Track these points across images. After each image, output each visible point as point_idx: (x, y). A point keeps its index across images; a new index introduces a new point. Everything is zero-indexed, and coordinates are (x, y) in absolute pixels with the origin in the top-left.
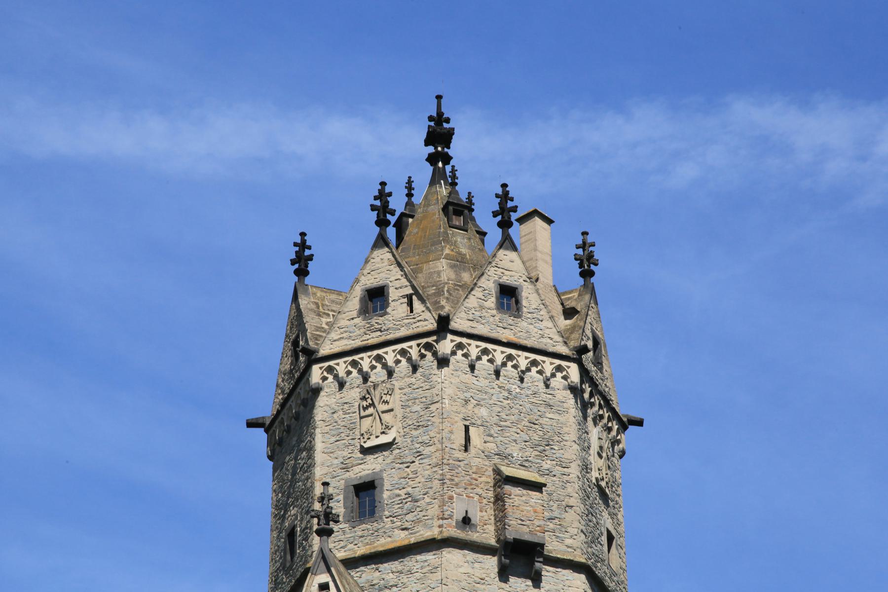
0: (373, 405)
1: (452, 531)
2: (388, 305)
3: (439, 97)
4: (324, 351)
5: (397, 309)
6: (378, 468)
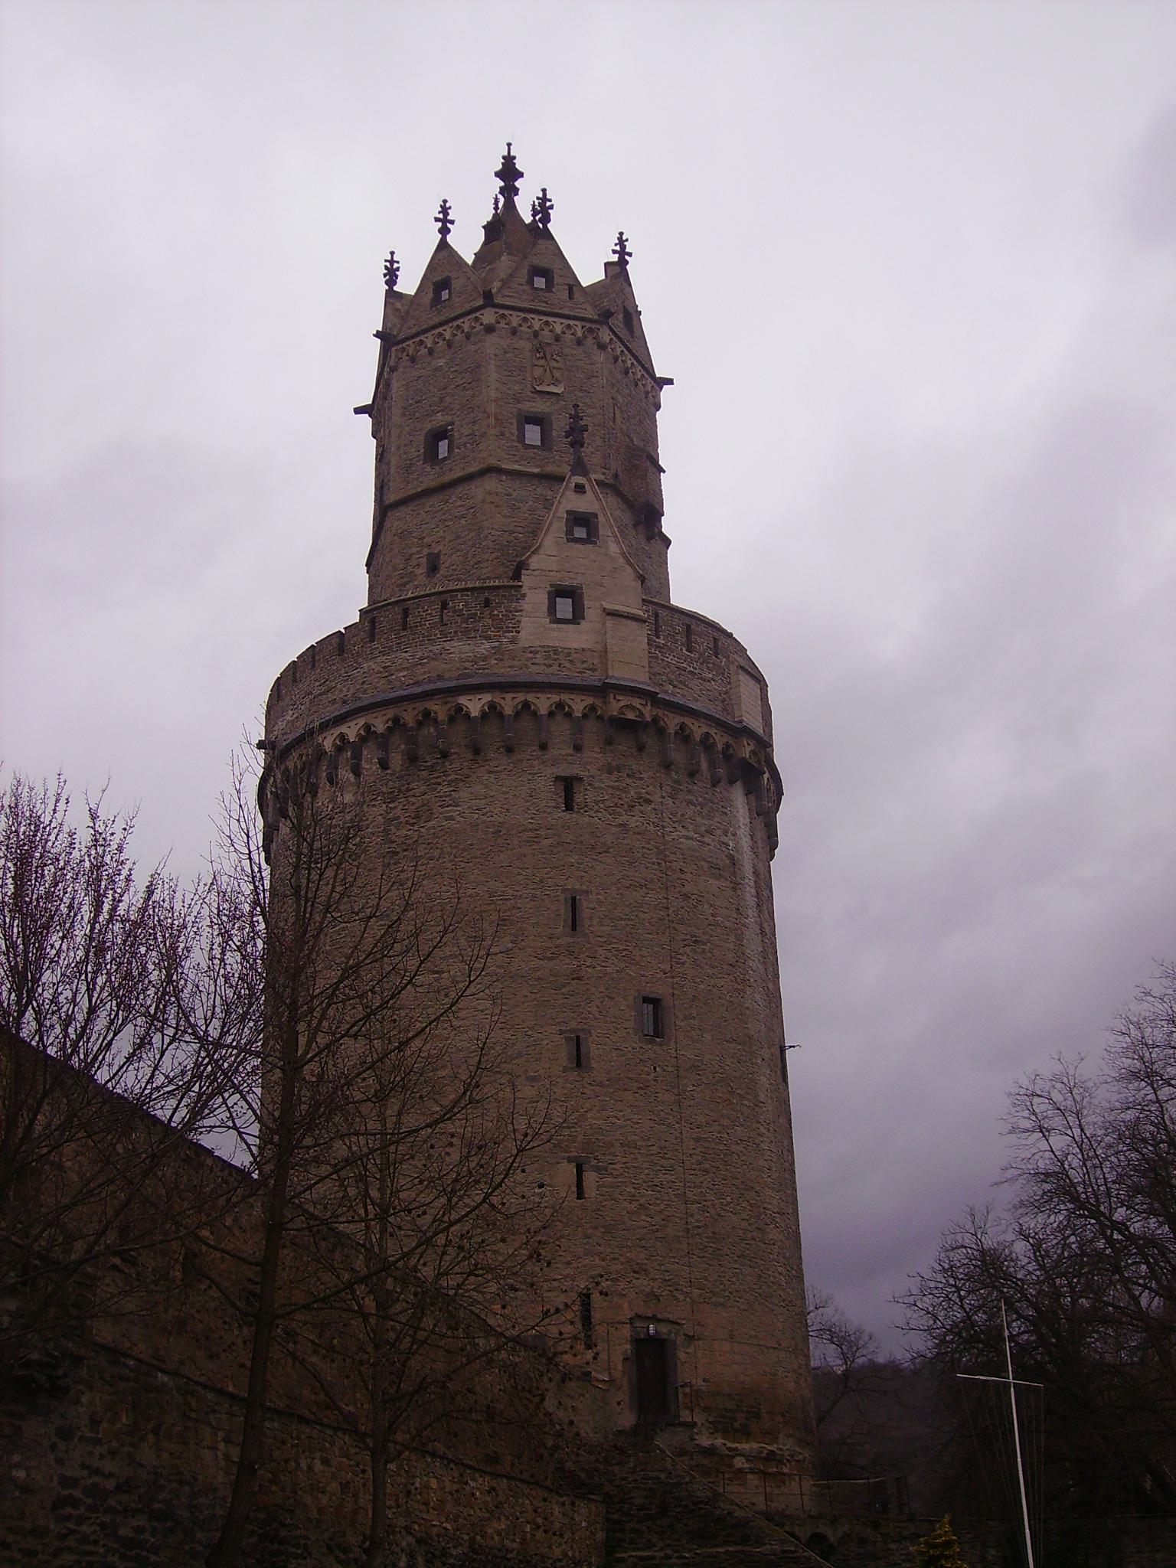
0: (544, 357)
3: (509, 145)
4: (498, 300)
6: (547, 410)
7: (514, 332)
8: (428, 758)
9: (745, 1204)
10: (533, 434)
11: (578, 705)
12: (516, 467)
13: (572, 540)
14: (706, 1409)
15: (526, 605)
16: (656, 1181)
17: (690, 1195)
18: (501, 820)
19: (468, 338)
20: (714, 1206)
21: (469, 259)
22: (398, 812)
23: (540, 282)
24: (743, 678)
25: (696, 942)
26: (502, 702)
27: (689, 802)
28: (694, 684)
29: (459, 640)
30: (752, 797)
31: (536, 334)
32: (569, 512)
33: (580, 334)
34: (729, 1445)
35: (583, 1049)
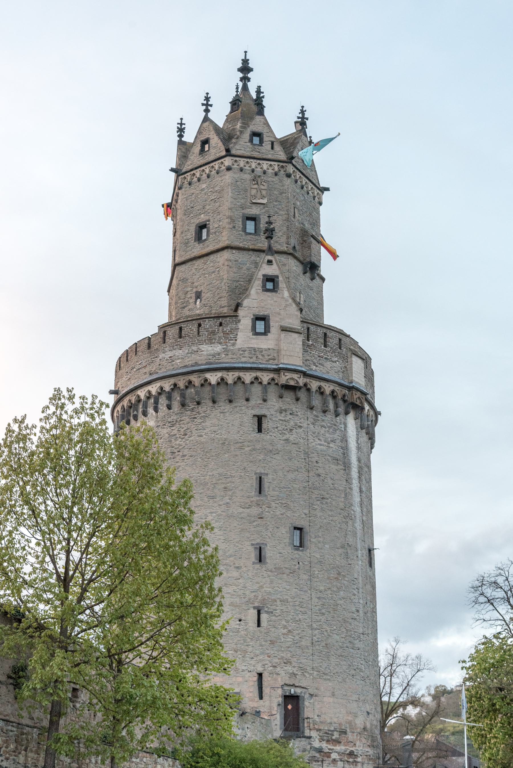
0: (257, 184)
1: (291, 251)
2: (263, 143)
3: (246, 52)
5: (267, 146)
6: (258, 213)
7: (241, 170)
8: (190, 404)
9: (344, 630)
10: (250, 226)
11: (265, 378)
13: (266, 290)
14: (319, 730)
15: (240, 326)
16: (297, 619)
17: (315, 626)
18: (225, 437)
19: (218, 173)
20: (327, 631)
22: (175, 432)
23: (256, 140)
24: (355, 359)
25: (322, 498)
26: (227, 377)
27: (322, 426)
28: (328, 364)
29: (206, 344)
30: (359, 421)
33: (276, 169)
34: (330, 747)
35: (263, 554)
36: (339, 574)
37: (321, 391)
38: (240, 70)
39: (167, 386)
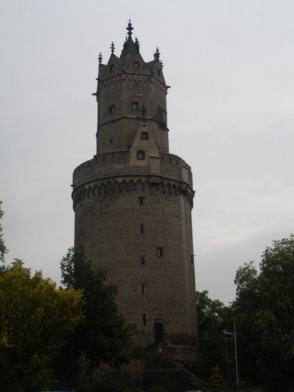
1: (153, 118)
4: (126, 72)
5: (142, 68)
7: (130, 80)
10: (134, 107)
11: (144, 180)
12: (131, 116)
13: (143, 139)
21: (119, 57)
23: (136, 65)
24: (183, 169)
27: (170, 201)
30: (185, 197)
31: (135, 80)
32: (142, 132)
33: (146, 79)
36: (178, 268)
37: (168, 185)
38: (127, 29)
39: (99, 184)
